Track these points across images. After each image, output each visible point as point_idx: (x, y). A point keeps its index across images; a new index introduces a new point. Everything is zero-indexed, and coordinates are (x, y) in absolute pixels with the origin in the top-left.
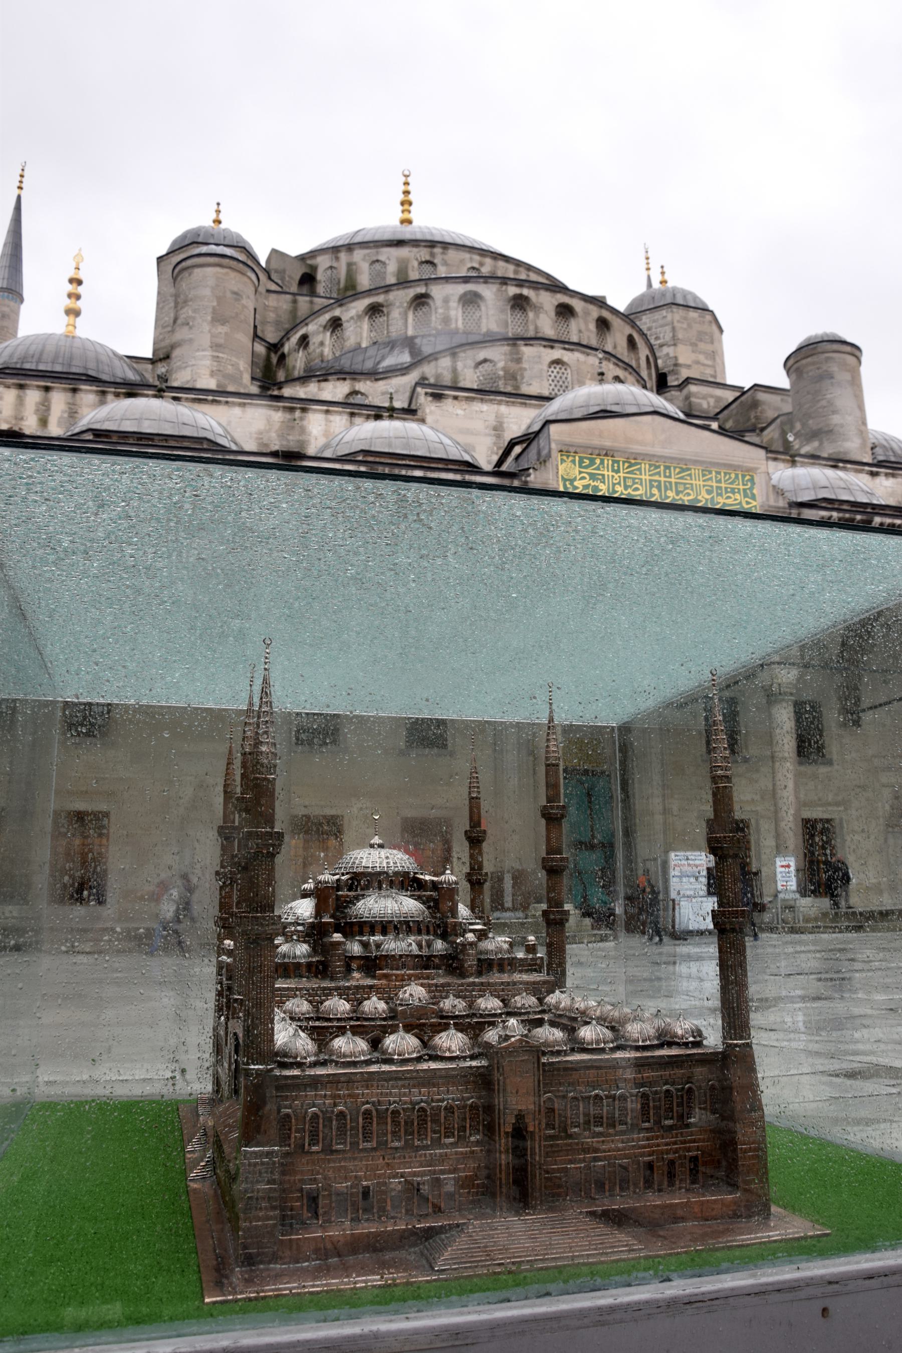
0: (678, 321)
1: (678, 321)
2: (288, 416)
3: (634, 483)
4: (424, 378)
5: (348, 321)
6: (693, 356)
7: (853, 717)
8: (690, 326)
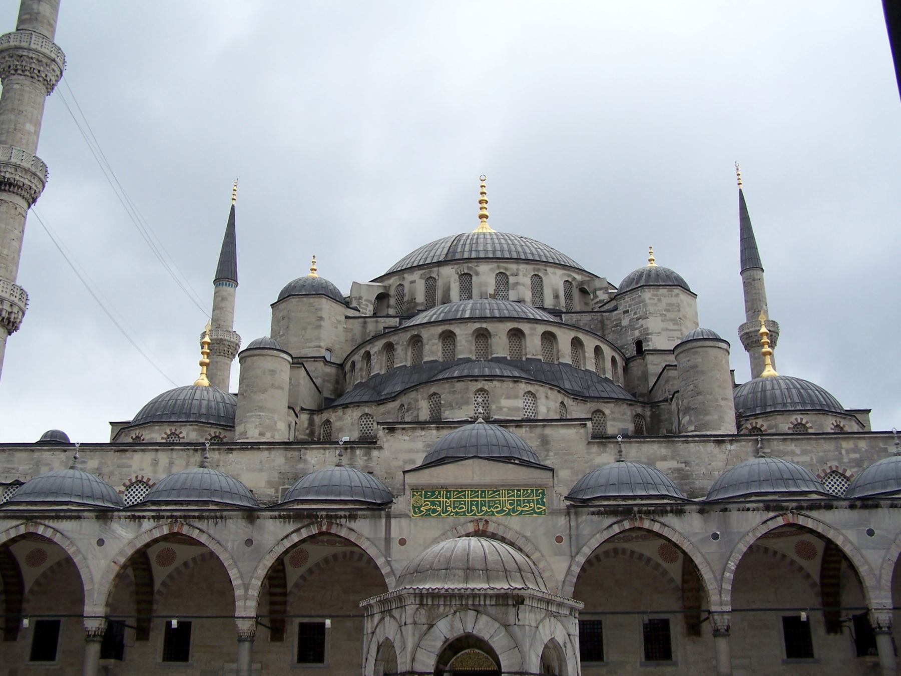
0: (650, 299)
1: (650, 299)
2: (296, 453)
4: (402, 405)
6: (662, 325)
7: (694, 629)
8: (659, 300)
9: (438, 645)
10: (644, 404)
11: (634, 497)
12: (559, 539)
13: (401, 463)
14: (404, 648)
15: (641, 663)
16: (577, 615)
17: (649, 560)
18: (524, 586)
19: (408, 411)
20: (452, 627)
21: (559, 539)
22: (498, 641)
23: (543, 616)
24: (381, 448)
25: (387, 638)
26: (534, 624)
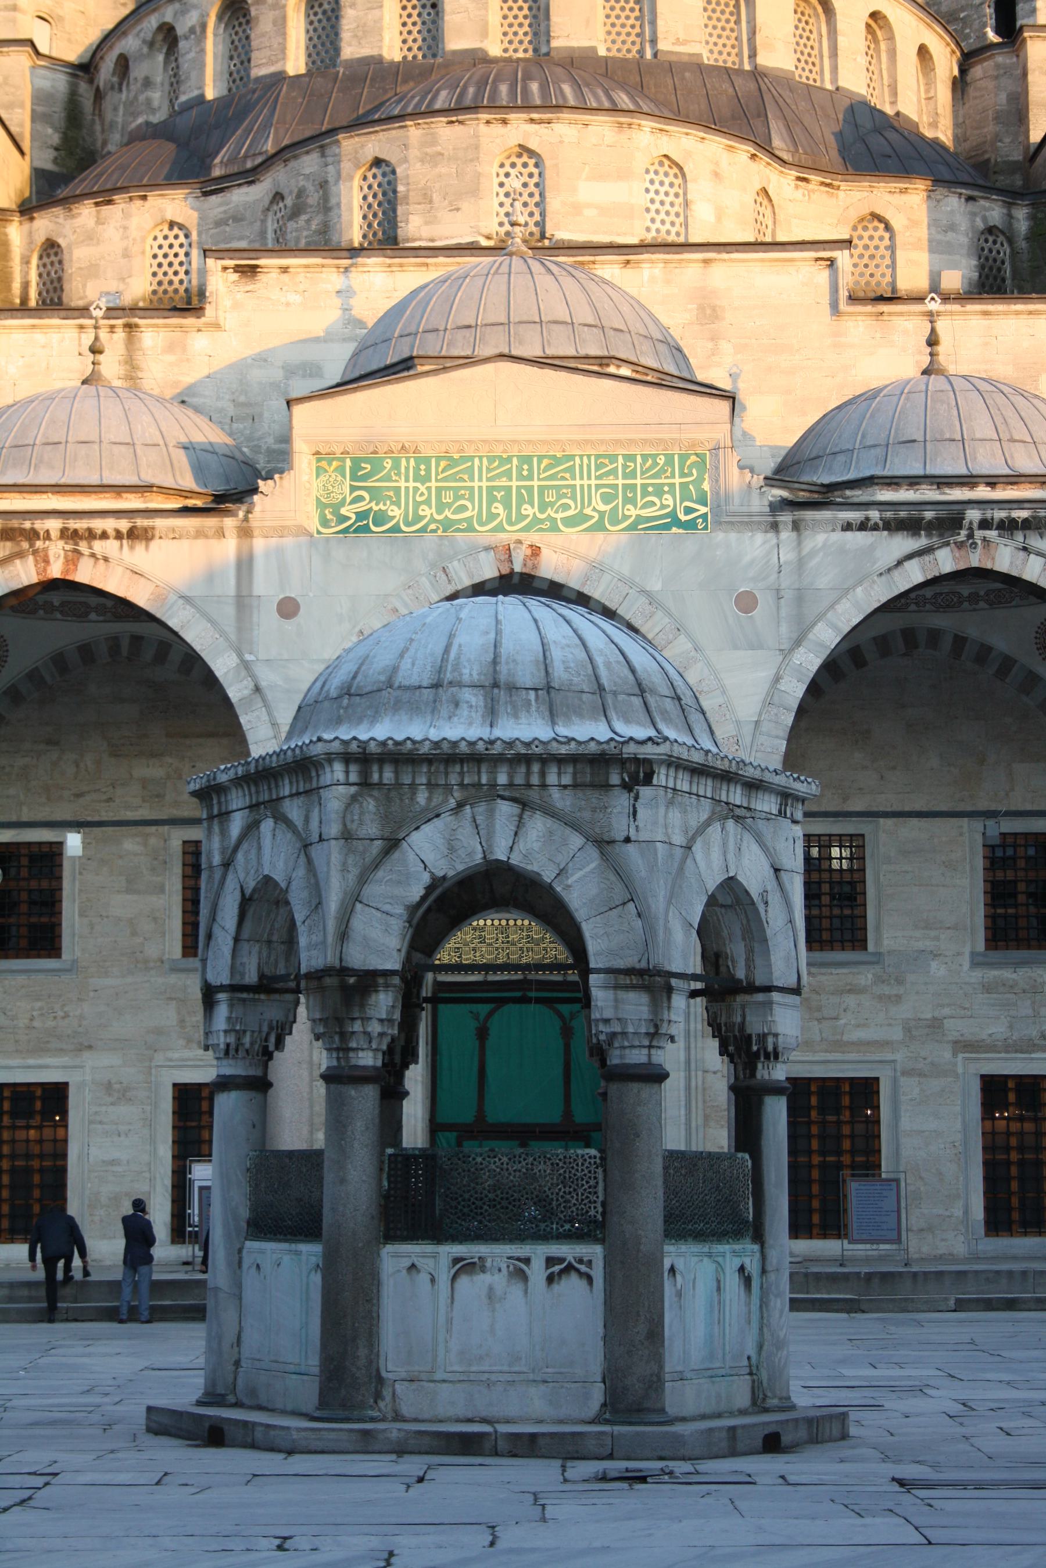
3: (457, 498)
4: (278, 196)
5: (186, 38)
9: (416, 892)
10: (1011, 196)
11: (969, 481)
12: (746, 602)
13: (278, 375)
14: (317, 905)
15: (973, 954)
16: (799, 815)
17: (1007, 664)
18: (652, 733)
19: (296, 212)
20: (452, 849)
21: (746, 602)
22: (581, 889)
23: (704, 816)
24: (217, 326)
25: (268, 880)
26: (678, 839)
